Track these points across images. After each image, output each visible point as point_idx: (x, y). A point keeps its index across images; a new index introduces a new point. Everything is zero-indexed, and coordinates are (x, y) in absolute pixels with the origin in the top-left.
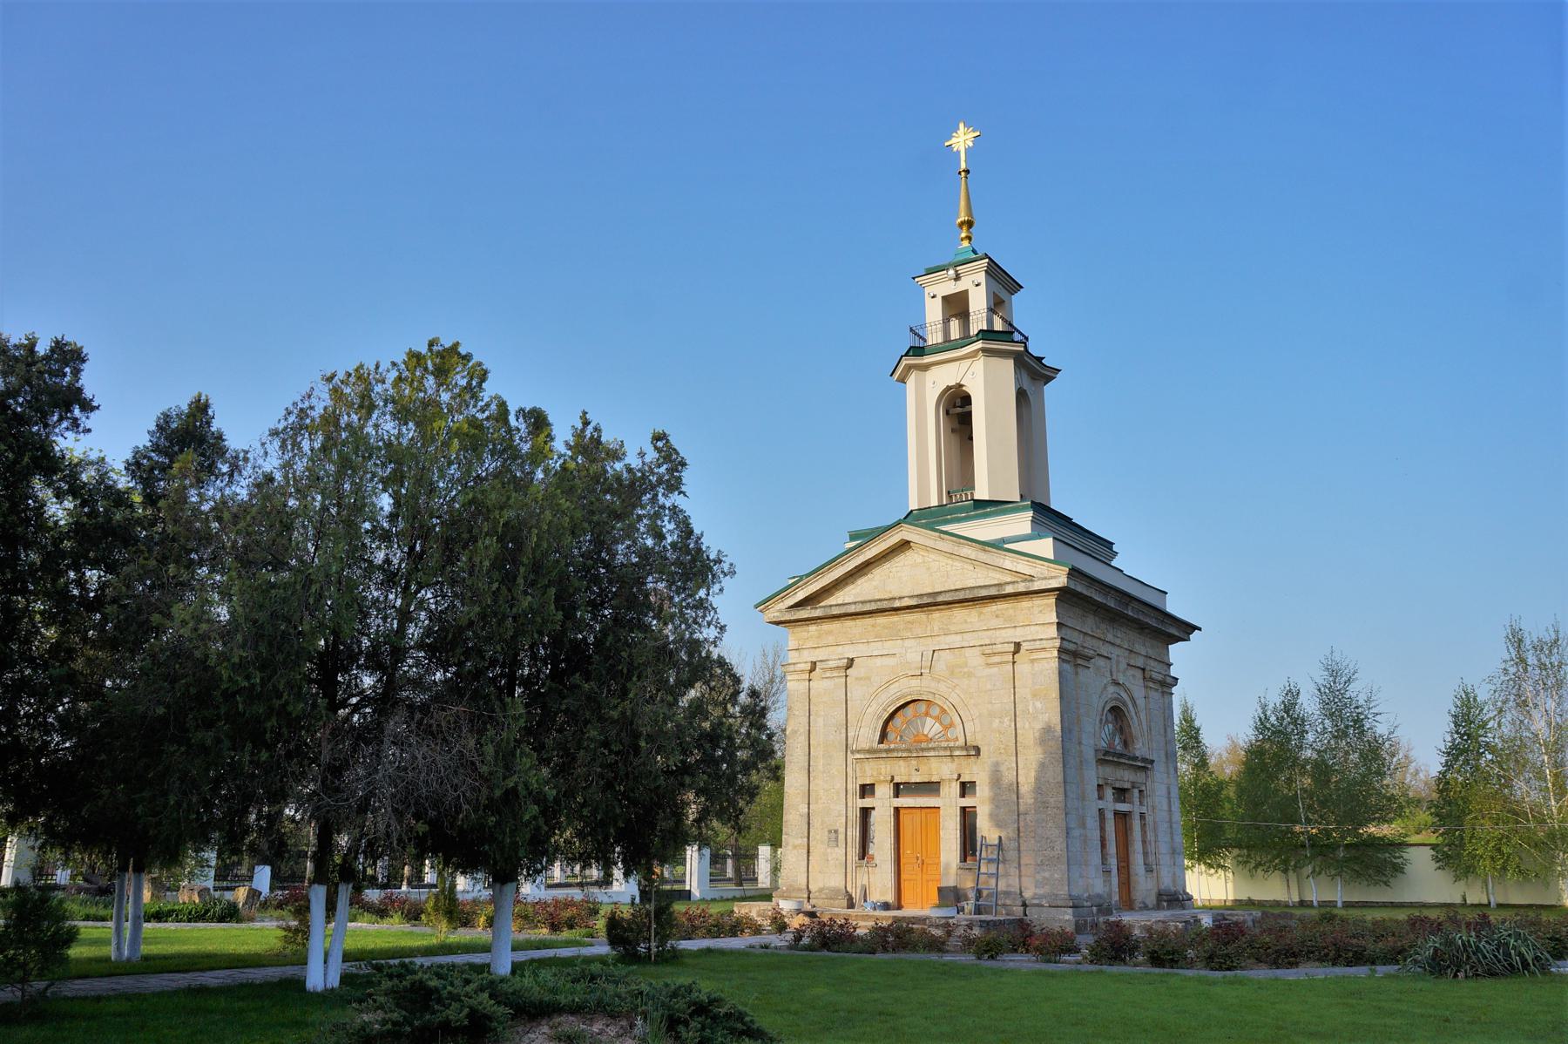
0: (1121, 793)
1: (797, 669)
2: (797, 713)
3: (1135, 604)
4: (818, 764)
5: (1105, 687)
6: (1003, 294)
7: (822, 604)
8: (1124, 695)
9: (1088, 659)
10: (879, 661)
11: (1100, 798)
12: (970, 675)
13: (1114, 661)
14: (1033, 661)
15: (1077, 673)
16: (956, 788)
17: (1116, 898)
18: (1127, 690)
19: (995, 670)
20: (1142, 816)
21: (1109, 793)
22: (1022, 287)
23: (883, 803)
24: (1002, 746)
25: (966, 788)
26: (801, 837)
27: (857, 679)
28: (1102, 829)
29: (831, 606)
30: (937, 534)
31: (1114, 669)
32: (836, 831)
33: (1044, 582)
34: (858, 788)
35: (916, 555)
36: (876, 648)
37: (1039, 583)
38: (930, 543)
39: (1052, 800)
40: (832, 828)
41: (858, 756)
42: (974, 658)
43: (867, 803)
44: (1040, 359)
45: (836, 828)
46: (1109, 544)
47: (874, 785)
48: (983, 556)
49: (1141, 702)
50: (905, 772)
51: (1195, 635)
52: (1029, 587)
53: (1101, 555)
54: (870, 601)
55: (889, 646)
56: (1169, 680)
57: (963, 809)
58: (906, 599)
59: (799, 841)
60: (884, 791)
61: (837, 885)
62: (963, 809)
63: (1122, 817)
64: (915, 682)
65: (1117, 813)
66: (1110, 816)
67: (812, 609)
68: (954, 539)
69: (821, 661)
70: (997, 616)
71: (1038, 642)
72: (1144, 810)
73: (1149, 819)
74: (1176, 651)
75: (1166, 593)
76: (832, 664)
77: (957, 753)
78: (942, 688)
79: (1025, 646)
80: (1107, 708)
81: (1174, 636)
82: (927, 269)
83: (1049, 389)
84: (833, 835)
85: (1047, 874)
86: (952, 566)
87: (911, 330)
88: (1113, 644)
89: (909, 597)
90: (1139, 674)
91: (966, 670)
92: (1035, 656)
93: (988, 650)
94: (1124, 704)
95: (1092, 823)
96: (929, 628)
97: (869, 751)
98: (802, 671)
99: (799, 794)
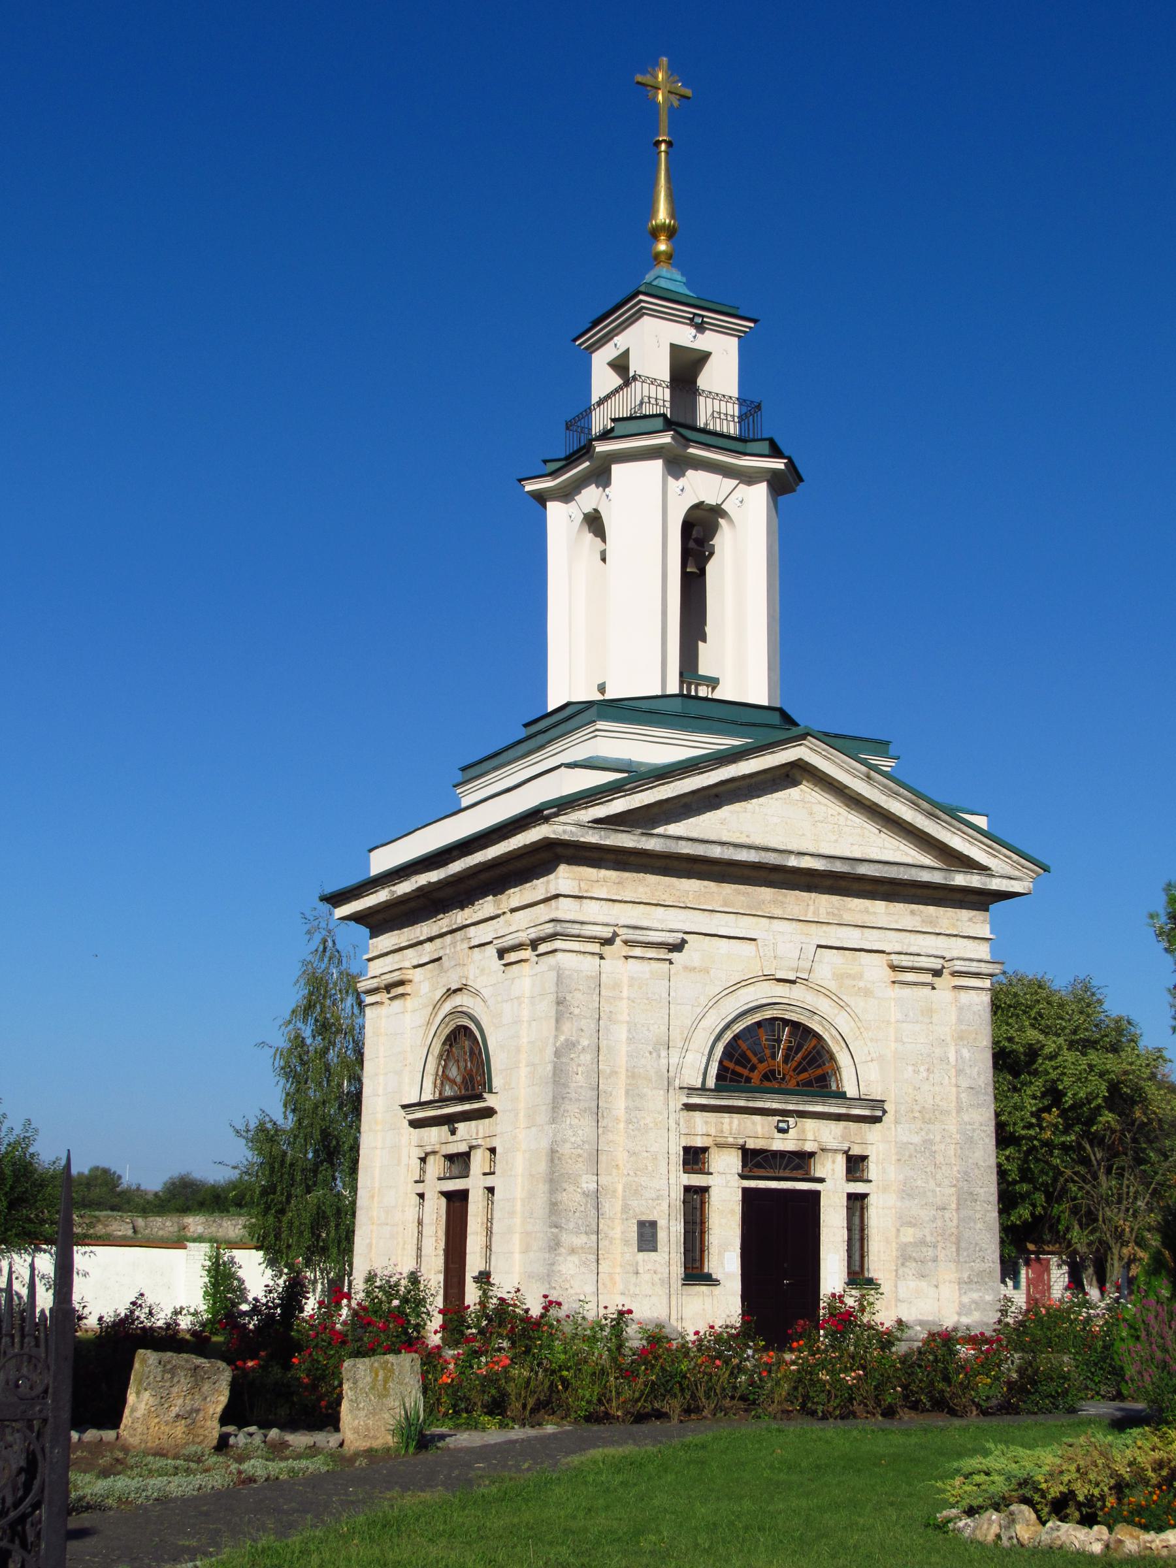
1: (583, 933)
2: (576, 1011)
7: (660, 830)
12: (867, 993)
19: (907, 991)
24: (917, 1108)
25: (856, 1165)
26: (586, 1233)
27: (686, 968)
30: (864, 769)
32: (653, 1224)
33: (1005, 881)
34: (682, 1153)
37: (998, 880)
39: (982, 1190)
40: (644, 1218)
45: (651, 1218)
52: (985, 884)
54: (750, 847)
57: (850, 1196)
59: (580, 1240)
61: (656, 1315)
62: (850, 1196)
67: (643, 834)
78: (823, 1006)
84: (648, 1230)
85: (975, 1296)
86: (847, 819)
91: (861, 984)
96: (811, 908)
98: (592, 939)
99: (579, 1156)
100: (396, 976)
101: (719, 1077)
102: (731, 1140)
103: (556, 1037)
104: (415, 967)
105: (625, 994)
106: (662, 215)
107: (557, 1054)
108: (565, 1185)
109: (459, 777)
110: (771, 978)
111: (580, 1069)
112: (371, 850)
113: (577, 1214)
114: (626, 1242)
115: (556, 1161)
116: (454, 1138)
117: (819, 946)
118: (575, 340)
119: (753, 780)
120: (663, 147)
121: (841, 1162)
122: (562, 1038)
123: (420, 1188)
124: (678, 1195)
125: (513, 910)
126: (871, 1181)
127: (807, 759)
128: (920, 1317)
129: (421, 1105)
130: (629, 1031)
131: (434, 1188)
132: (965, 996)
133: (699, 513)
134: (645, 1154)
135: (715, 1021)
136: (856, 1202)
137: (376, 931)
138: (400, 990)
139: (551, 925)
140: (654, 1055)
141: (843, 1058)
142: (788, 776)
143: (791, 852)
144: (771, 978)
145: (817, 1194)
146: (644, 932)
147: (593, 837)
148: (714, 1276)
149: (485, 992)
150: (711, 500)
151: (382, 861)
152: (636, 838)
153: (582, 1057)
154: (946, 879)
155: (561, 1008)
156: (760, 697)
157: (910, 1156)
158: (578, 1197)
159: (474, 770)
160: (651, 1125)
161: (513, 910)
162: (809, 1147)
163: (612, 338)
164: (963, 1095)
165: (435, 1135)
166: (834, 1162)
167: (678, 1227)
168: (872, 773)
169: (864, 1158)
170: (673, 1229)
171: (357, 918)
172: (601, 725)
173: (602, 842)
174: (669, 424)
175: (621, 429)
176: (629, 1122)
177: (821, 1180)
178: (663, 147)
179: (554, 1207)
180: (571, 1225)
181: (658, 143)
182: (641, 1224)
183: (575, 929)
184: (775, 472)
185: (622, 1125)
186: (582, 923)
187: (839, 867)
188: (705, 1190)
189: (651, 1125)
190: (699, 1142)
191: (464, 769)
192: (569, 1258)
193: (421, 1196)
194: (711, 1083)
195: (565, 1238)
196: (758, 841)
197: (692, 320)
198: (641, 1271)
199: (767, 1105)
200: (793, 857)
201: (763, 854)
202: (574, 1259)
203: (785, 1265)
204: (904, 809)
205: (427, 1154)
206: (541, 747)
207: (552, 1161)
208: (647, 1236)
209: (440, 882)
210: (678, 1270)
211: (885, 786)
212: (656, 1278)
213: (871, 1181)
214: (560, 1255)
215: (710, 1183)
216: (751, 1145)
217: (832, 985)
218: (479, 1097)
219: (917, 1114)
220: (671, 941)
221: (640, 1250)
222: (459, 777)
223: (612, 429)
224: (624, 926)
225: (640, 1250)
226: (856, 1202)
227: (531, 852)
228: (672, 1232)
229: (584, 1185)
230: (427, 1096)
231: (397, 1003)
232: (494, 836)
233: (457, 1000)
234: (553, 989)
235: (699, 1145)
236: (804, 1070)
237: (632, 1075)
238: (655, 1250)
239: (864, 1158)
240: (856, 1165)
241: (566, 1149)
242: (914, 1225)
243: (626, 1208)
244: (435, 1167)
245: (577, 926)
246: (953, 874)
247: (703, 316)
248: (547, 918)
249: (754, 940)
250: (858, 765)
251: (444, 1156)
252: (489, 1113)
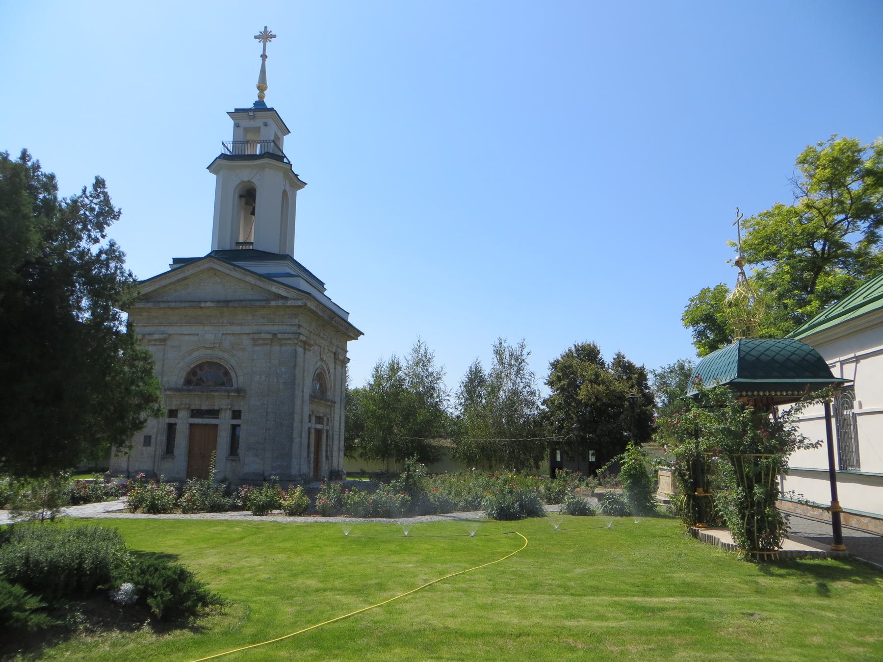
0: (319, 420)
3: (337, 318)
5: (317, 362)
6: (279, 134)
8: (325, 367)
9: (311, 345)
10: (187, 338)
11: (310, 421)
13: (322, 348)
14: (281, 345)
15: (305, 353)
16: (229, 414)
17: (311, 474)
18: (327, 364)
20: (327, 431)
21: (313, 419)
22: (290, 132)
23: (183, 421)
25: (236, 414)
27: (171, 347)
28: (309, 438)
29: (159, 302)
31: (322, 353)
32: (150, 437)
36: (187, 329)
37: (291, 302)
38: (227, 271)
40: (147, 435)
41: (168, 393)
42: (246, 341)
43: (172, 420)
44: (297, 176)
46: (322, 284)
47: (177, 411)
48: (259, 283)
49: (332, 371)
51: (361, 337)
53: (850, 298)
55: (194, 329)
56: (346, 360)
58: (208, 303)
60: (183, 414)
63: (319, 432)
64: (209, 352)
65: (316, 429)
66: (313, 431)
68: (243, 271)
69: (149, 334)
70: (264, 318)
71: (286, 335)
72: (328, 428)
73: (330, 433)
74: (351, 345)
75: (348, 313)
76: (156, 336)
77: (232, 394)
78: (226, 356)
79: (279, 336)
80: (317, 373)
81: (351, 337)
82: (236, 109)
83: (300, 193)
87: (223, 144)
88: (323, 339)
89: (212, 302)
90: (332, 356)
92: (283, 342)
93: (256, 336)
94: (325, 371)
95: (305, 435)
97: (177, 390)
110: (204, 347)
117: (223, 334)
127: (212, 266)
132: (284, 348)
144: (204, 347)
150: (246, 179)
162: (216, 408)
164: (281, 386)
167: (163, 438)
170: (159, 438)
182: (145, 437)
198: (144, 453)
204: (251, 279)
215: (177, 422)
216: (193, 407)
221: (144, 446)
225: (144, 446)
226: (234, 427)
238: (150, 445)
240: (236, 414)
249: (198, 334)
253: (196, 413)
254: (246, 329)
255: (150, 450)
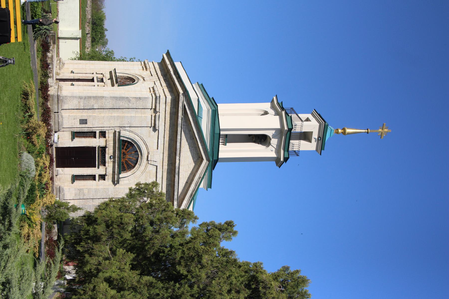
2: (138, 102)
4: (116, 113)
25: (103, 177)
30: (202, 176)
32: (86, 123)
35: (197, 159)
40: (88, 121)
45: (88, 122)
50: (109, 152)
67: (182, 118)
78: (142, 168)
84: (85, 122)
91: (148, 178)
99: (102, 104)
100: (148, 67)
101: (123, 140)
102: (108, 143)
103: (131, 97)
104: (150, 71)
105: (143, 115)
106: (348, 131)
107: (127, 98)
108: (95, 100)
109: (200, 83)
110: (148, 153)
111: (124, 104)
112: (181, 62)
113: (88, 103)
114: (82, 116)
115: (101, 98)
116: (107, 80)
117: (157, 166)
118: (315, 110)
119: (198, 148)
120: (367, 131)
121: (103, 173)
122: (131, 99)
123: (95, 73)
124: (94, 130)
125: (163, 89)
126: (99, 181)
127: (204, 161)
128: (65, 194)
129: (115, 73)
130: (134, 116)
131: (95, 76)
133: (269, 139)
134: (103, 121)
135: (137, 139)
136: (93, 177)
137: (160, 64)
138: (145, 68)
139: (159, 96)
140: (128, 123)
141: (129, 173)
142: (199, 157)
143: (180, 158)
144: (148, 153)
145: (95, 167)
146: (158, 120)
147: (180, 105)
148: (74, 140)
149: (143, 85)
151: (178, 65)
152: (181, 116)
153: (126, 104)
154: (176, 199)
155: (139, 98)
156: (221, 155)
157: (105, 191)
158: (92, 103)
159: (202, 87)
160: (111, 122)
161: (163, 89)
162: (107, 164)
163: (314, 118)
165: (108, 76)
166: (103, 171)
167: (86, 130)
168: (201, 179)
169: (104, 180)
171: (163, 59)
172: (210, 110)
173: (179, 107)
174: (290, 130)
175: (289, 118)
176: (111, 116)
177: (98, 168)
178: (367, 131)
179: (90, 97)
180: (85, 102)
181: (368, 129)
182: (86, 120)
183: (158, 102)
184: (280, 159)
185: (110, 115)
186: (159, 103)
187: (177, 170)
188: (95, 137)
189: (111, 122)
190: (107, 135)
191: (202, 84)
192: (77, 102)
193: (93, 74)
194: (122, 138)
195: (82, 100)
196: (182, 149)
197: (319, 137)
199: (117, 153)
200: (179, 158)
201: (179, 150)
202: (77, 103)
203: (77, 158)
204: (193, 188)
205: (103, 75)
206: (206, 99)
207: (101, 97)
208: (83, 122)
209: (171, 74)
210: (76, 130)
211: (198, 182)
212: (73, 124)
213: (99, 181)
214: (78, 99)
216: (107, 149)
217: (147, 170)
218: (117, 82)
219: (116, 193)
220: (156, 126)
221: (80, 120)
222: (200, 83)
223: (288, 116)
224: (159, 115)
225: (80, 120)
226: (93, 177)
227: (176, 90)
228: (84, 128)
229: (95, 105)
230: (118, 74)
231: (142, 68)
232: (181, 83)
233: (142, 79)
234: (143, 97)
235: (106, 135)
236: (126, 163)
237: (123, 117)
238: (80, 124)
239: (104, 180)
240: (103, 177)
241: (104, 100)
242: (88, 193)
243: (90, 116)
244: (101, 76)
245: (159, 102)
246: (177, 201)
247: (320, 140)
248: (160, 95)
250: (203, 175)
251: (103, 78)
252: (113, 85)
253: (103, 149)
254: (159, 181)
255: (78, 125)
